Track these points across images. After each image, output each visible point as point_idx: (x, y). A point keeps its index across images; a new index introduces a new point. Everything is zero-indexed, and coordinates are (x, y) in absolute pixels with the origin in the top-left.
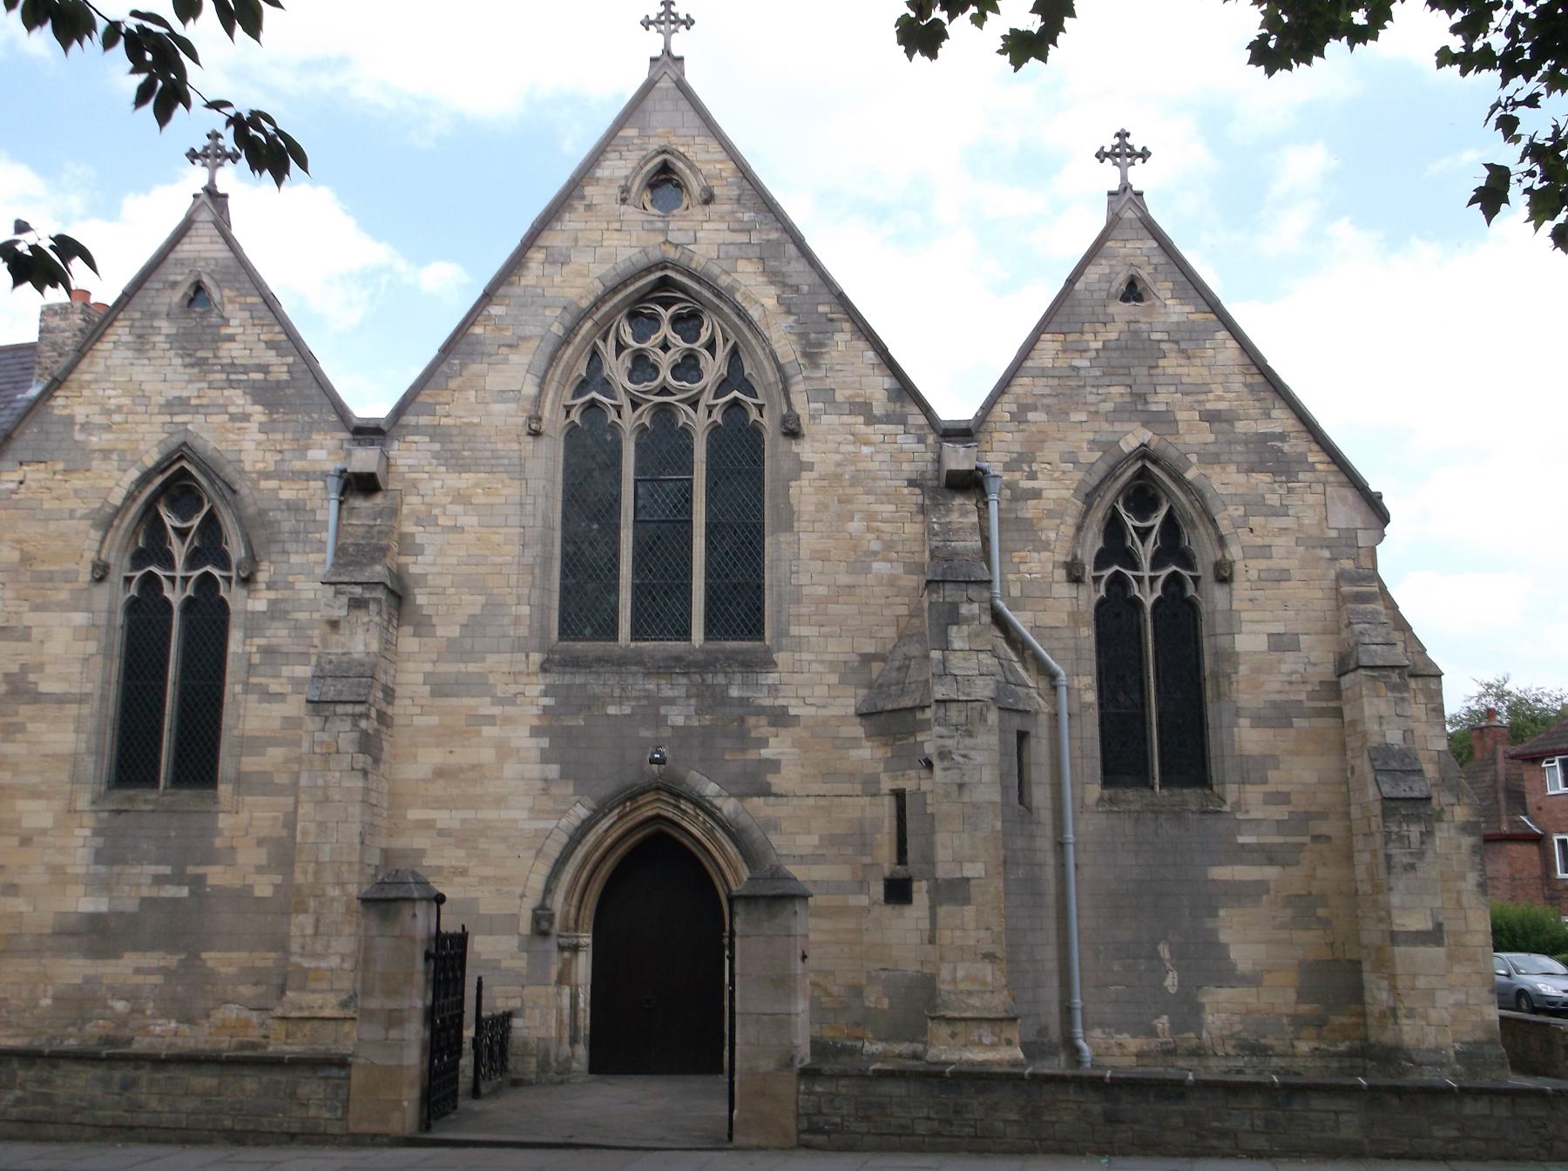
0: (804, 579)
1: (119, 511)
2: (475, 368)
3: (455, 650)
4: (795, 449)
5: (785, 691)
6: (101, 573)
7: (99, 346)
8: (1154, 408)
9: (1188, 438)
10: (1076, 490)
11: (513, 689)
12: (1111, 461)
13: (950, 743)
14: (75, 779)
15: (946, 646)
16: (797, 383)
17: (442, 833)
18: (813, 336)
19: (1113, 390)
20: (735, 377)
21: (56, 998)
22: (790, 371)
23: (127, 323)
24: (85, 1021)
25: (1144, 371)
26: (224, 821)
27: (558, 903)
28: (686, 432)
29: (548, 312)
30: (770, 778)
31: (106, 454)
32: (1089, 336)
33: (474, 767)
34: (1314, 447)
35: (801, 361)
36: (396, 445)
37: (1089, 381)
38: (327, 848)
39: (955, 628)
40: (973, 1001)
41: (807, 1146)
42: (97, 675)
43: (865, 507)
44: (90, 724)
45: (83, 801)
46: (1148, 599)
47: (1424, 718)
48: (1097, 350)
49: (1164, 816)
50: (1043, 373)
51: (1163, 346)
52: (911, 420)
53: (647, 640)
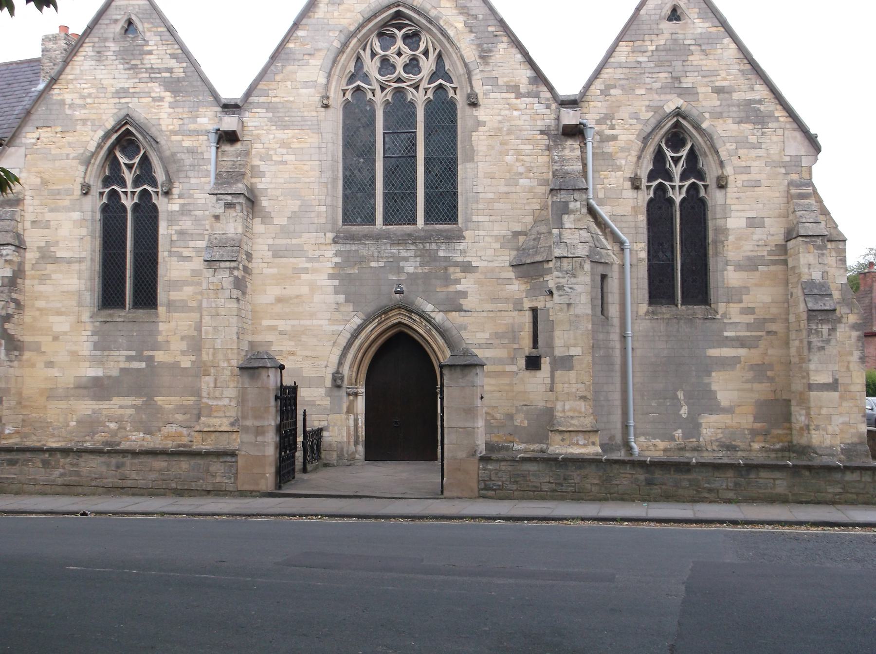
0: (480, 189)
1: (94, 155)
2: (290, 68)
3: (284, 231)
4: (475, 113)
5: (469, 253)
6: (86, 190)
7: (76, 58)
8: (684, 85)
9: (704, 104)
10: (638, 135)
11: (318, 253)
12: (658, 117)
13: (561, 280)
14: (80, 304)
15: (561, 227)
16: (476, 74)
17: (281, 333)
18: (485, 45)
19: (660, 75)
20: (440, 72)
21: (78, 422)
22: (472, 67)
23: (91, 45)
24: (95, 434)
25: (680, 63)
26: (162, 327)
27: (346, 371)
28: (412, 104)
29: (331, 34)
30: (462, 301)
31: (84, 121)
32: (648, 43)
33: (297, 296)
34: (779, 107)
35: (479, 61)
36: (247, 114)
37: (647, 70)
38: (219, 341)
39: (566, 216)
40: (574, 422)
41: (484, 497)
42: (88, 246)
43: (515, 147)
44: (86, 274)
45: (86, 316)
46: (678, 197)
47: (835, 265)
48: (652, 51)
49: (683, 321)
50: (620, 66)
51: (692, 48)
52: (542, 95)
53: (392, 225)
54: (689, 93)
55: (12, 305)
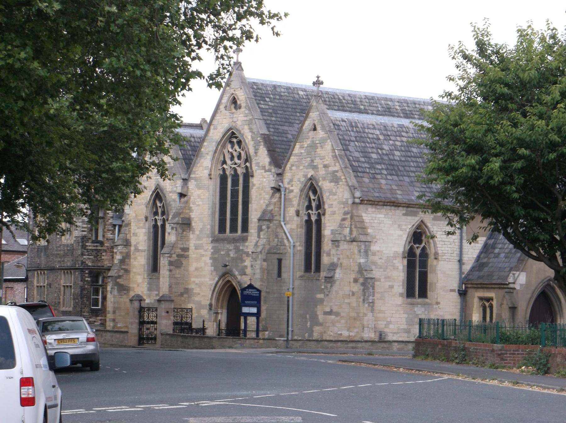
1: (149, 202)
2: (202, 160)
11: (207, 247)
17: (196, 284)
27: (213, 302)
32: (305, 143)
54: (315, 168)
55: (122, 271)
